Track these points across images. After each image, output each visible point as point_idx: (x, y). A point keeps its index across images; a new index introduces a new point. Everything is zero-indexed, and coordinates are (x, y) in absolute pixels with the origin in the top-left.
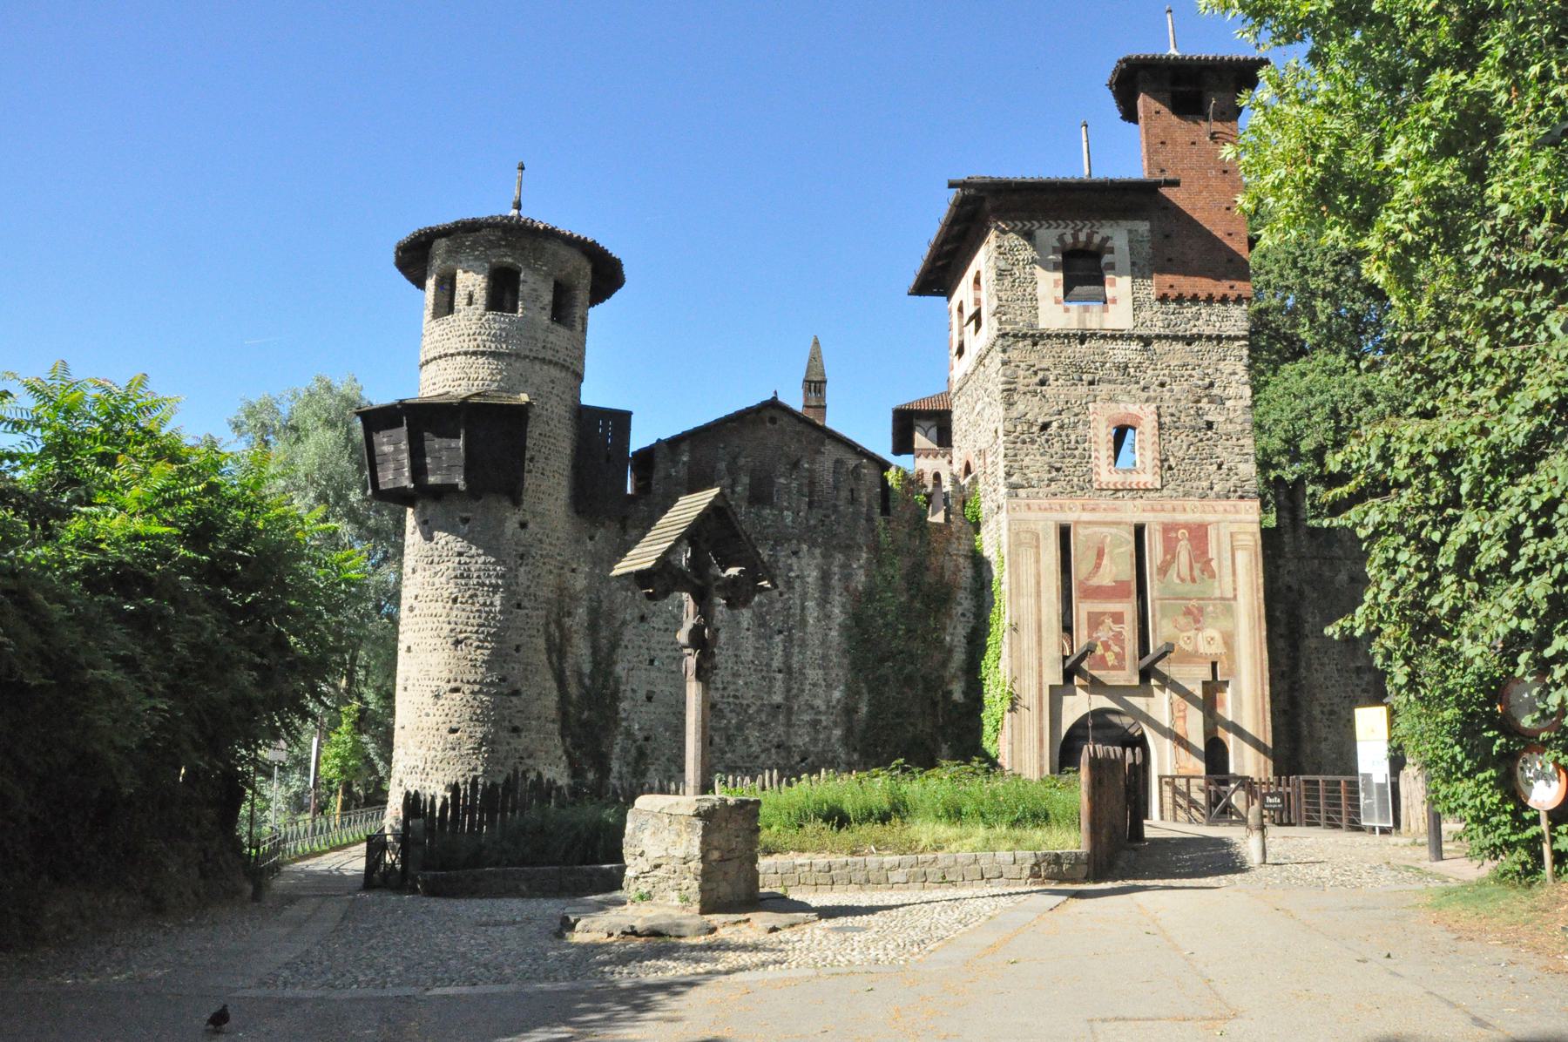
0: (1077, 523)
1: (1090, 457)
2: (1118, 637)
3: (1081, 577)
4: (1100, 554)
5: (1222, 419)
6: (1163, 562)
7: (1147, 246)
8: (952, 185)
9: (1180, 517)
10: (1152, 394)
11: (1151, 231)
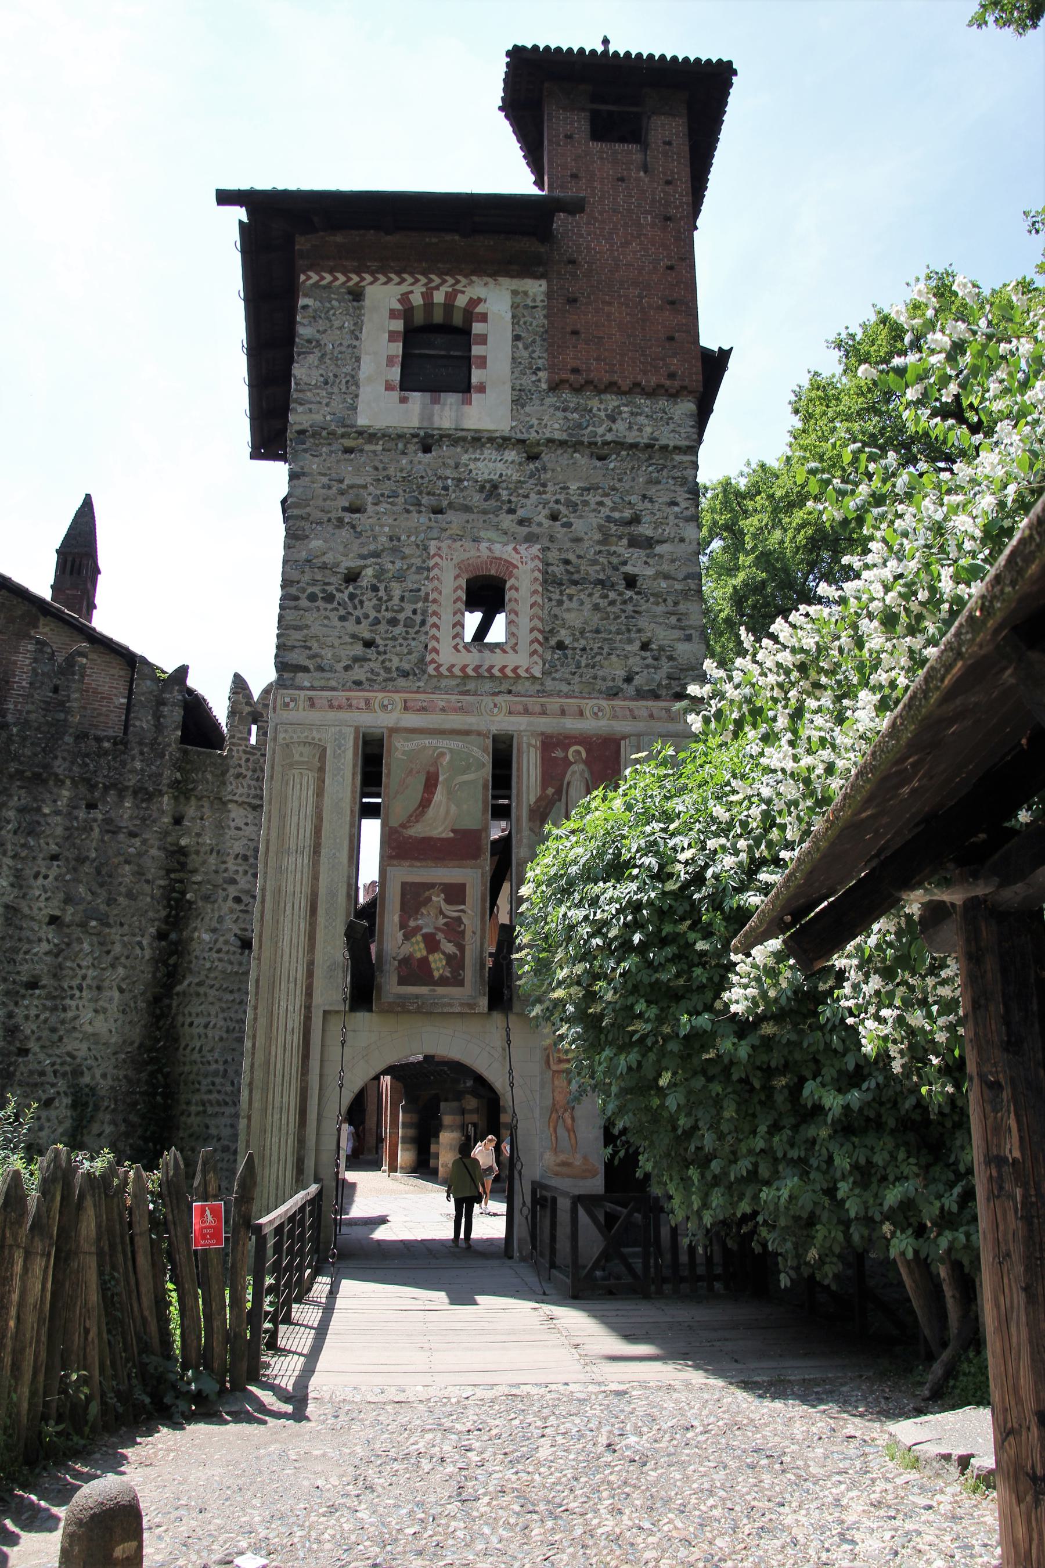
0: (393, 730)
1: (423, 623)
2: (454, 929)
3: (394, 823)
4: (431, 784)
5: (650, 572)
6: (538, 800)
7: (540, 314)
8: (225, 198)
9: (572, 725)
10: (535, 529)
11: (549, 294)
